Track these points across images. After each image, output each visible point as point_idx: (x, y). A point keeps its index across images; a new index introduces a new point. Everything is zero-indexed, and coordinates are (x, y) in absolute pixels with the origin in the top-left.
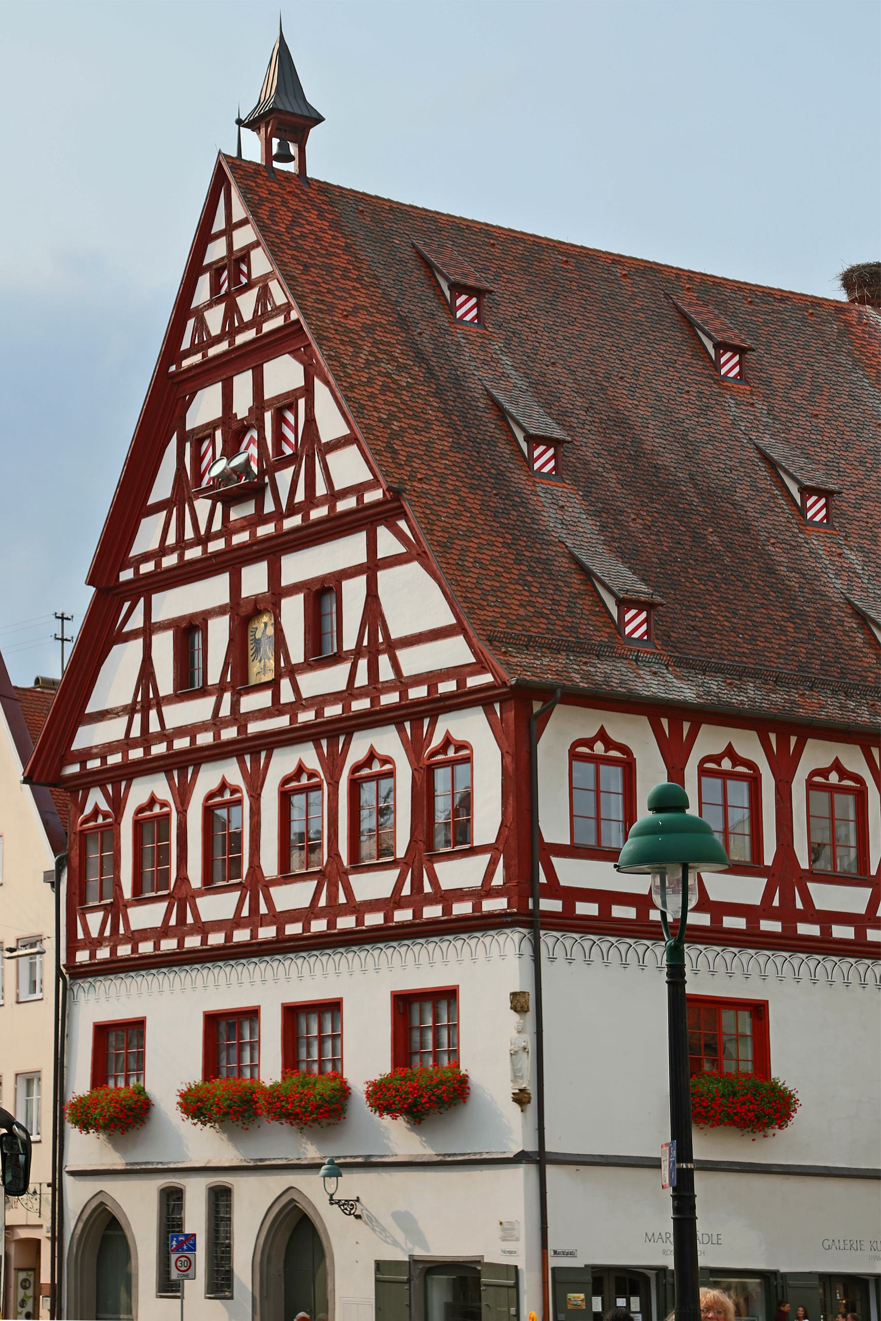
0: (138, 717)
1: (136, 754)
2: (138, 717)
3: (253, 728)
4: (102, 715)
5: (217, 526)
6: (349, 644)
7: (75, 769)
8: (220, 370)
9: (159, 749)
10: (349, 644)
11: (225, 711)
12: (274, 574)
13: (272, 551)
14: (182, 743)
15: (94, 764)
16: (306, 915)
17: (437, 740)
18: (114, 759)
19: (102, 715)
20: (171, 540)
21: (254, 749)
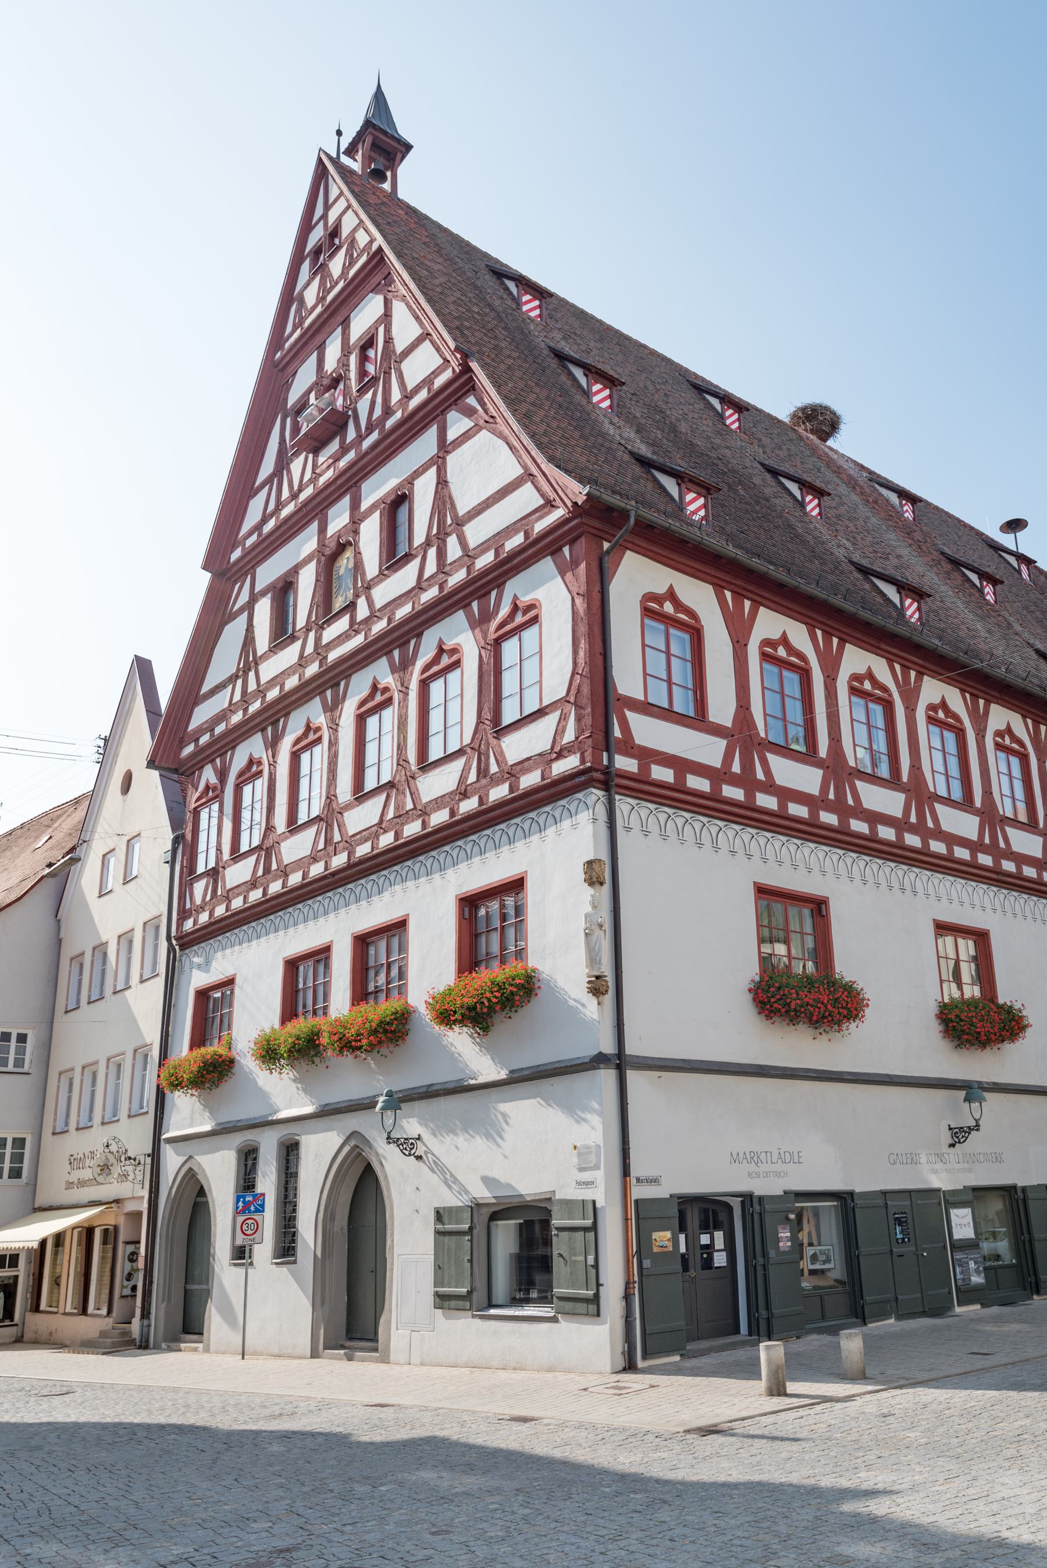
0: (239, 682)
1: (237, 718)
2: (239, 682)
3: (333, 656)
4: (213, 692)
5: (308, 475)
6: (419, 539)
7: (190, 749)
8: (313, 339)
9: (255, 706)
10: (419, 539)
11: (310, 649)
12: (355, 505)
13: (348, 483)
14: (273, 694)
15: (204, 739)
16: (372, 833)
17: (504, 611)
18: (220, 729)
19: (213, 692)
20: (272, 506)
21: (330, 682)
